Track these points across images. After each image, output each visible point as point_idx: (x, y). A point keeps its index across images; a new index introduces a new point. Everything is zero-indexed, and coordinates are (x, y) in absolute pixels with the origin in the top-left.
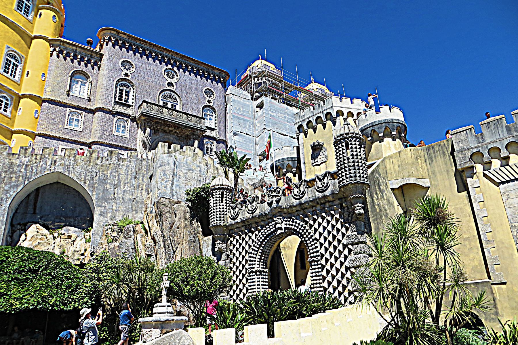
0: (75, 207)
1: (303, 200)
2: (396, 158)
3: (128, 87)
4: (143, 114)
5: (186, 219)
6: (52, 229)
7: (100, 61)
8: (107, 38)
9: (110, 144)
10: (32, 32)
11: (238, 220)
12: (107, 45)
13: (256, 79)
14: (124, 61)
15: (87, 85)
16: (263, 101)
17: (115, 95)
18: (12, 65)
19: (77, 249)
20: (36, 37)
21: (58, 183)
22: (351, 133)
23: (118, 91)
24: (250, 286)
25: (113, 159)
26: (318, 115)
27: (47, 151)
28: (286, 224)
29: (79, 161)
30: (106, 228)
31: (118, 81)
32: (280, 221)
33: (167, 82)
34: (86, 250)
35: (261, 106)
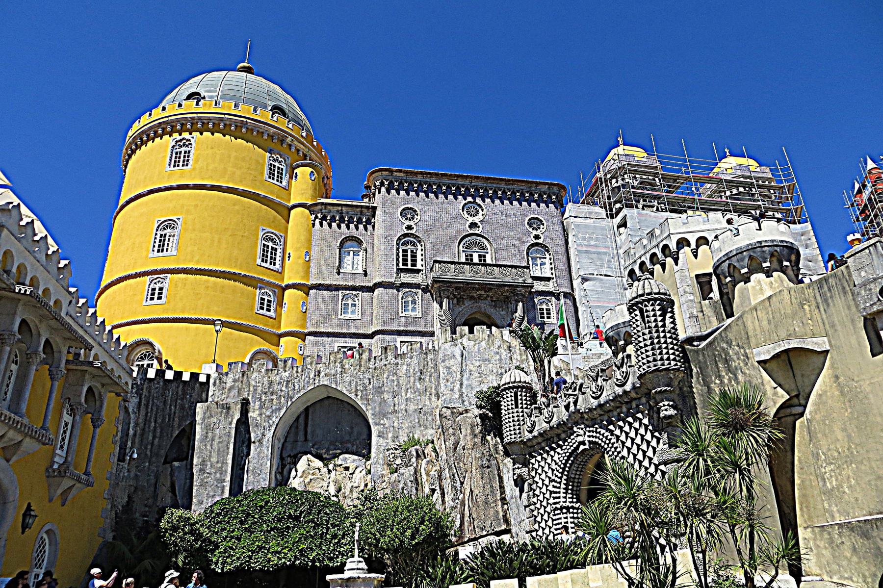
0: (352, 428)
1: (602, 400)
2: (765, 308)
3: (414, 245)
4: (435, 281)
5: (475, 436)
6: (326, 459)
7: (374, 216)
8: (378, 183)
9: (398, 331)
10: (289, 201)
11: (535, 433)
12: (379, 193)
13: (614, 181)
14: (404, 210)
15: (361, 253)
16: (625, 217)
17: (397, 260)
18: (270, 250)
19: (356, 485)
20: (294, 206)
21: (328, 397)
22: (655, 294)
23: (400, 254)
24: (556, 530)
25: (389, 358)
26: (653, 251)
27: (309, 360)
28: (589, 436)
29: (347, 366)
30: (387, 453)
31: (399, 239)
32: (582, 432)
33: (468, 224)
34: (366, 485)
35: (623, 224)
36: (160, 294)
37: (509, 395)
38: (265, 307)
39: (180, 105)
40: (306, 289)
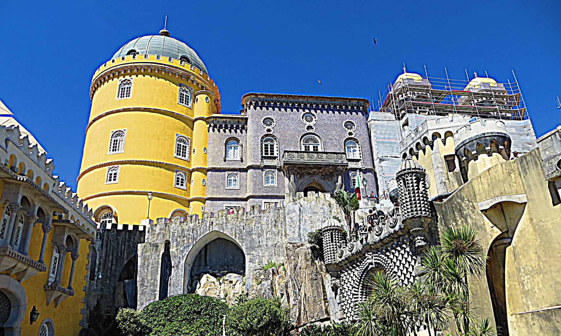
0: (234, 257)
1: (382, 237)
2: (486, 176)
3: (272, 141)
4: (285, 164)
5: (308, 260)
6: (218, 276)
7: (246, 124)
8: (248, 103)
9: (262, 196)
10: (193, 116)
11: (343, 258)
12: (249, 109)
13: (400, 96)
14: (265, 119)
15: (239, 148)
16: (407, 120)
17: (262, 151)
18: (182, 147)
19: (237, 292)
20: (196, 120)
21: (219, 238)
22: (413, 169)
23: (264, 147)
25: (256, 213)
26: (417, 141)
27: (206, 215)
28: (375, 259)
29: (229, 219)
30: (255, 272)
31: (262, 138)
32: (370, 257)
33: (306, 127)
34: (243, 292)
35: (406, 124)
36: (115, 177)
37: (328, 234)
38: (180, 183)
39: (123, 59)
40: (205, 171)
